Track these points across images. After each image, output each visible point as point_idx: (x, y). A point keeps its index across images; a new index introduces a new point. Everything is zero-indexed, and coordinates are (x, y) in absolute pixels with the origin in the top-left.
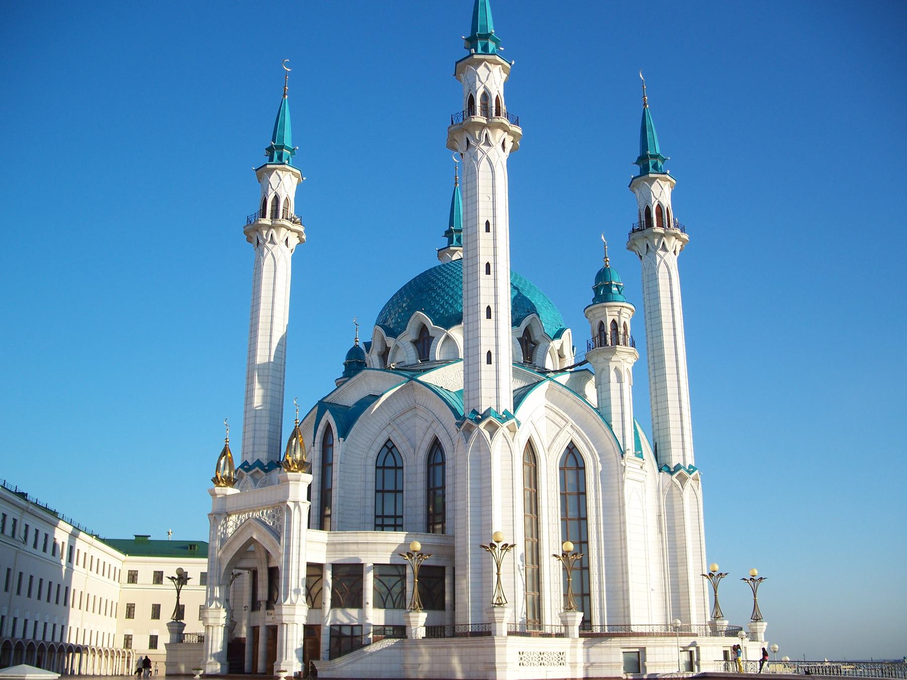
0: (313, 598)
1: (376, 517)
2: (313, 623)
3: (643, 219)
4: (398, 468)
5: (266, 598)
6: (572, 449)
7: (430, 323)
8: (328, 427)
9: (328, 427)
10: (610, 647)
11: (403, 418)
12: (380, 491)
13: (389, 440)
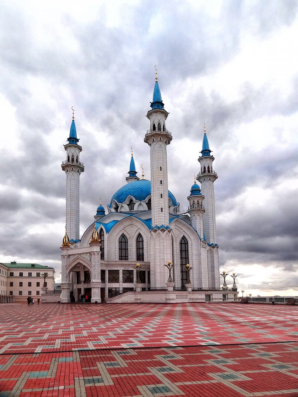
3: (203, 170)
4: (126, 242)
7: (134, 199)
8: (102, 229)
9: (102, 229)
10: (201, 294)
11: (128, 227)
13: (123, 234)
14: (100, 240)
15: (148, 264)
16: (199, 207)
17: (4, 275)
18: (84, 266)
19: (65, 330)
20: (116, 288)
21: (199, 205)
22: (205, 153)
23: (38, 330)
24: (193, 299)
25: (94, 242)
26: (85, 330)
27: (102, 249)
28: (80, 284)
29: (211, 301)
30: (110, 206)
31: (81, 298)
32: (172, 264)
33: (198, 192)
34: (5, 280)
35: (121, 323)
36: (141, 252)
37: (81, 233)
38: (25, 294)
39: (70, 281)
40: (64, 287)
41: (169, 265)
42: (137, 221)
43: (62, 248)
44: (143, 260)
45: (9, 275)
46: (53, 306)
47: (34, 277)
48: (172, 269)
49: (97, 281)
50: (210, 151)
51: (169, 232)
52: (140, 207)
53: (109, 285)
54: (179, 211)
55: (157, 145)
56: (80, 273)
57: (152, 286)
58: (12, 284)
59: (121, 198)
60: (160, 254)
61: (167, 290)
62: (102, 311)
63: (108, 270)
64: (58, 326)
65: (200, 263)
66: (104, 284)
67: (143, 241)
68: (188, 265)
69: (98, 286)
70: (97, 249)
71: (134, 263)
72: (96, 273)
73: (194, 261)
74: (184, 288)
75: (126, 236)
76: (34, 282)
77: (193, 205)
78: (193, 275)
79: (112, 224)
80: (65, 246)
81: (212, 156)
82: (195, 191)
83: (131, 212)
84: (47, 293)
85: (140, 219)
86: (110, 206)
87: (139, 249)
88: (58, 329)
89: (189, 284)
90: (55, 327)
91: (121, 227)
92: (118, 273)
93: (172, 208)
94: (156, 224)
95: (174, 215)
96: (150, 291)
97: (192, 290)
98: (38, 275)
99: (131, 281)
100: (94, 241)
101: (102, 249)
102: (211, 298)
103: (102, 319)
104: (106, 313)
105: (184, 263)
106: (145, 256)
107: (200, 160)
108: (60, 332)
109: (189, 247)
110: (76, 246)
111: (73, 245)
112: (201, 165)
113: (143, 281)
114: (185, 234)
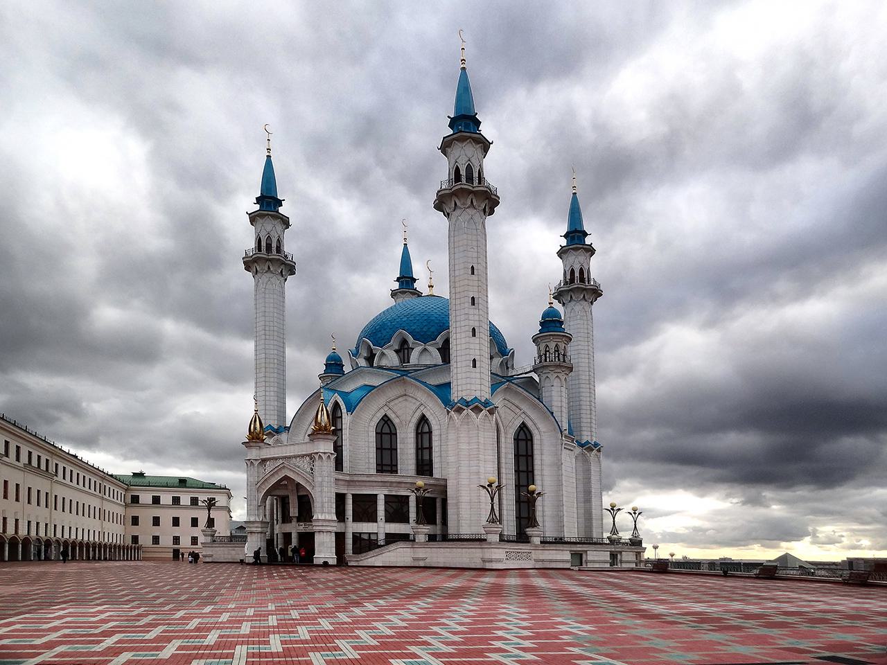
4: (393, 434)
8: (336, 405)
9: (336, 405)
11: (396, 401)
13: (386, 415)
14: (333, 428)
15: (443, 483)
16: (559, 360)
17: (119, 501)
18: (298, 484)
19: (257, 624)
20: (370, 534)
21: (559, 354)
22: (573, 238)
23: (194, 623)
24: (543, 561)
25: (319, 432)
26: (304, 624)
27: (338, 448)
28: (287, 523)
29: (584, 566)
30: (355, 352)
31: (287, 554)
32: (496, 484)
33: (558, 325)
34: (120, 511)
35: (386, 610)
36: (426, 457)
37: (291, 412)
38: (166, 541)
39: (265, 515)
40: (254, 529)
41: (490, 485)
42: (416, 386)
43: (248, 445)
44: (431, 475)
45: (129, 500)
46: (227, 569)
47: (185, 507)
48: (497, 494)
49: (328, 517)
50: (585, 234)
51: (491, 412)
52: (423, 357)
53: (353, 527)
54: (513, 368)
55: (465, 216)
56: (288, 499)
57: (452, 530)
58: (135, 521)
59: (380, 335)
60: (470, 463)
61: (486, 540)
62: (340, 583)
63: (353, 495)
64: (240, 614)
65: (559, 485)
66: (342, 524)
67: (430, 432)
68: (532, 487)
69: (329, 529)
70: (326, 447)
71: (409, 480)
72: (326, 500)
73: (546, 478)
74: (522, 538)
75: (392, 419)
76: (185, 516)
77: (545, 355)
78: (544, 509)
79: (359, 394)
80: (253, 438)
81: (590, 245)
82: (550, 323)
83: (403, 367)
84: (215, 541)
85: (424, 383)
86: (356, 354)
87: (422, 449)
88: (240, 622)
89: (535, 529)
90: (232, 617)
91: (382, 401)
92: (375, 502)
93: (498, 361)
94: (461, 395)
95: (500, 377)
96: (447, 543)
97: (541, 542)
98: (194, 501)
99: (405, 520)
100: (320, 430)
101: (338, 448)
102: (584, 560)
103: (342, 601)
104: (349, 587)
105: (523, 482)
106: (436, 465)
107: (562, 253)
108: (246, 628)
109: (535, 447)
110: (278, 441)
111: (271, 438)
112: (565, 266)
113: (432, 521)
114: (527, 419)
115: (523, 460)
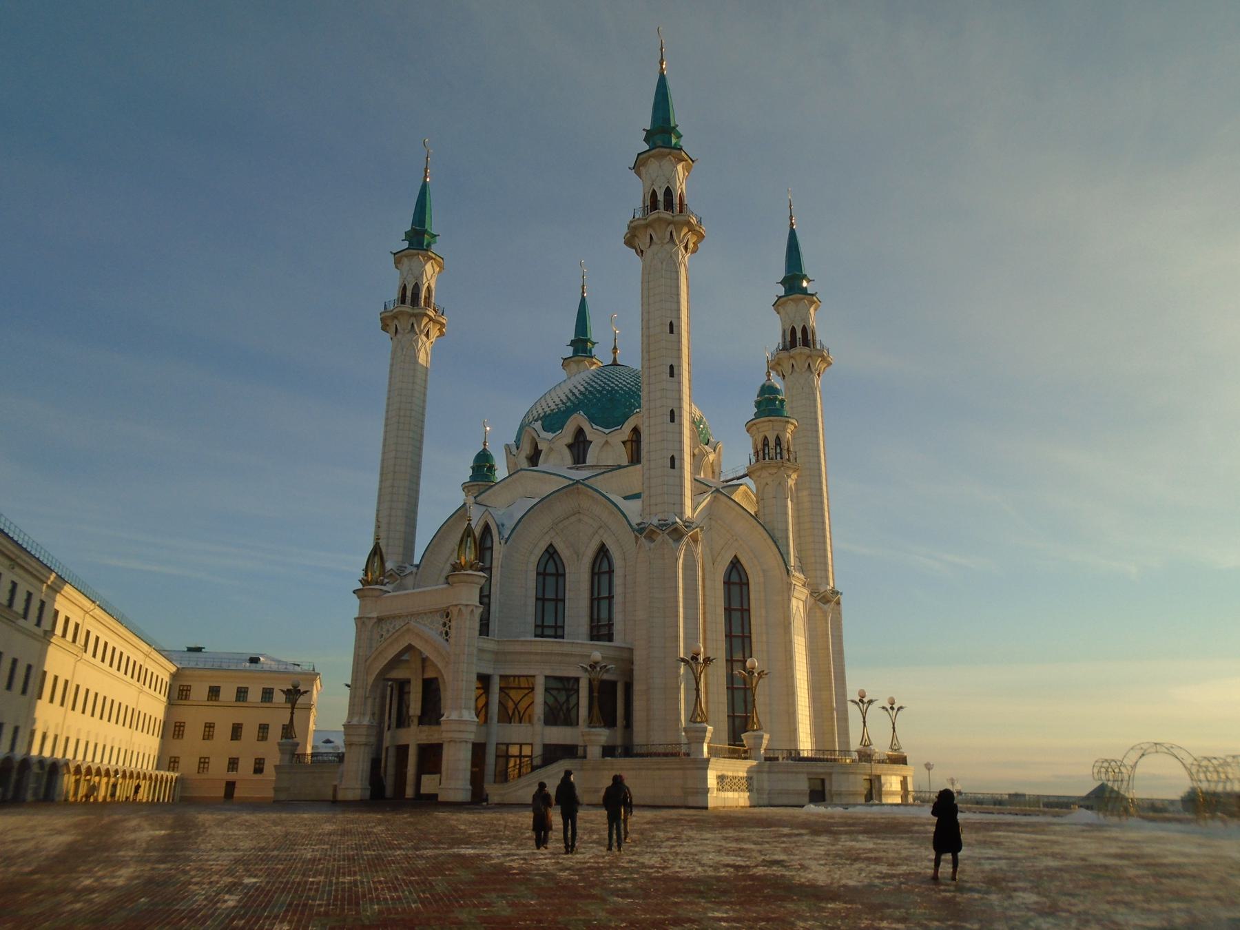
0: (483, 711)
1: (536, 626)
2: (478, 741)
3: (788, 338)
4: (560, 575)
5: (419, 712)
6: (736, 564)
12: (541, 600)
13: (551, 545)
18: (424, 660)
20: (521, 745)
27: (485, 598)
57: (639, 737)
67: (611, 572)
113: (610, 722)
115: (736, 616)
